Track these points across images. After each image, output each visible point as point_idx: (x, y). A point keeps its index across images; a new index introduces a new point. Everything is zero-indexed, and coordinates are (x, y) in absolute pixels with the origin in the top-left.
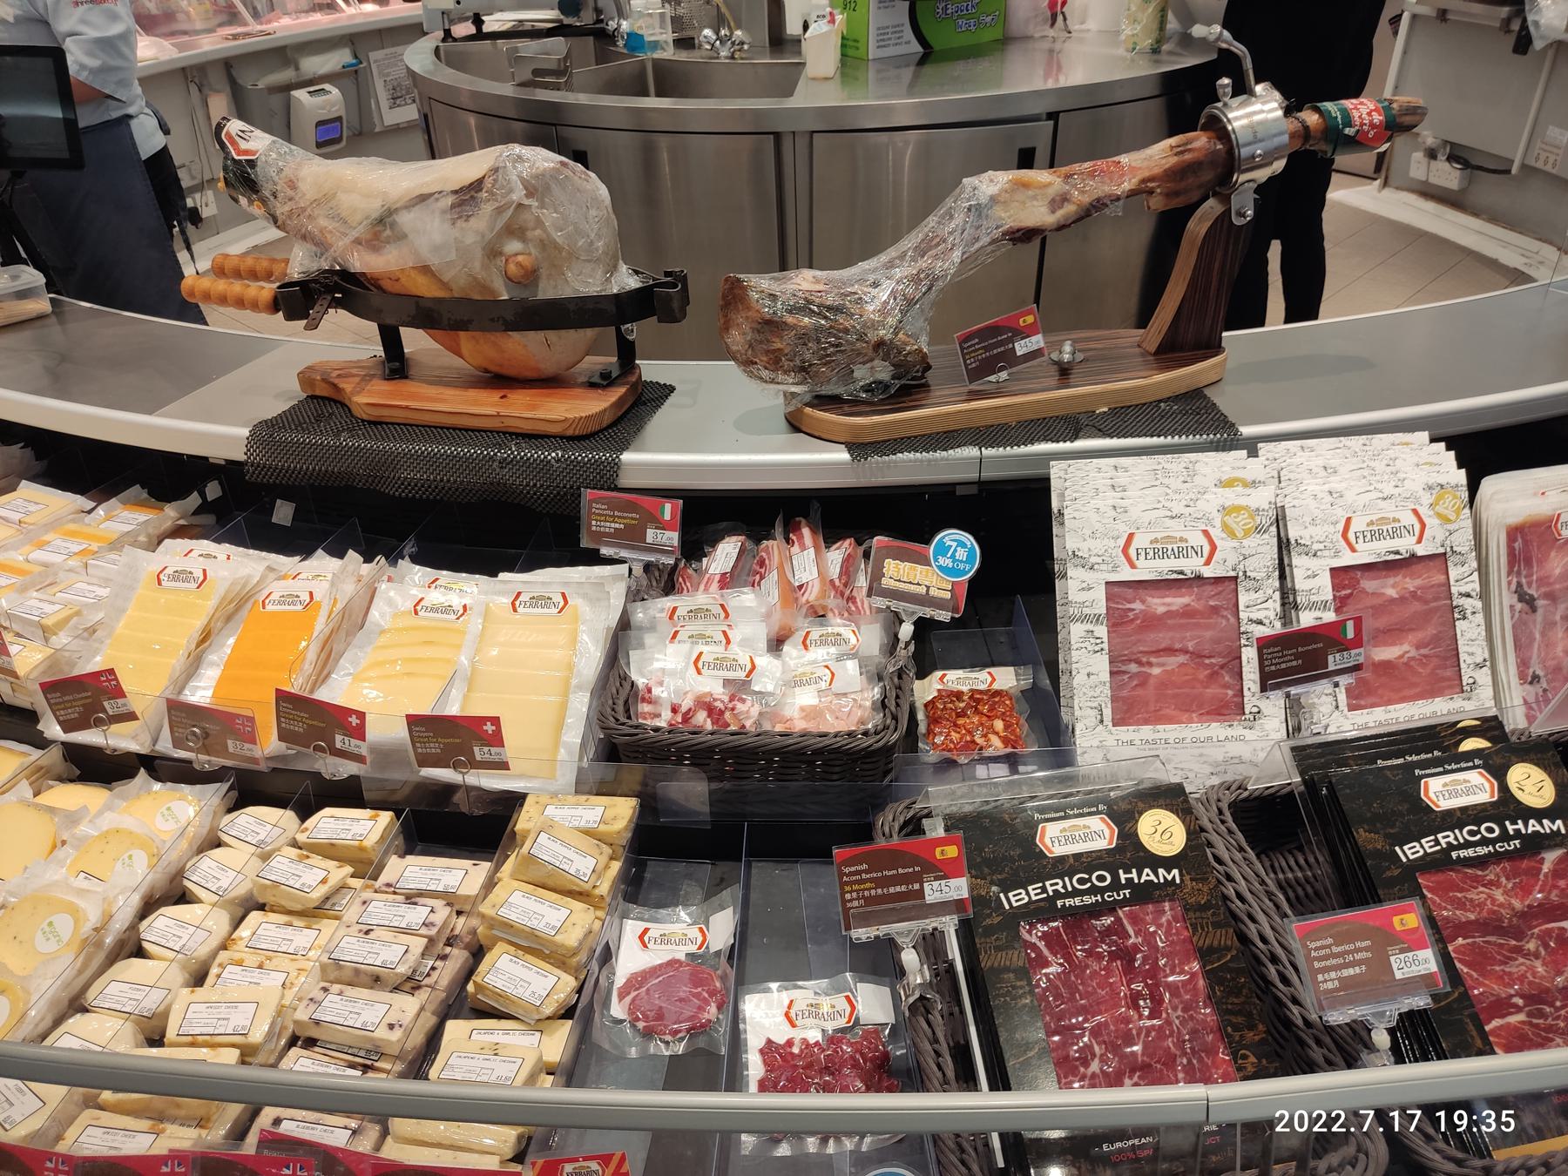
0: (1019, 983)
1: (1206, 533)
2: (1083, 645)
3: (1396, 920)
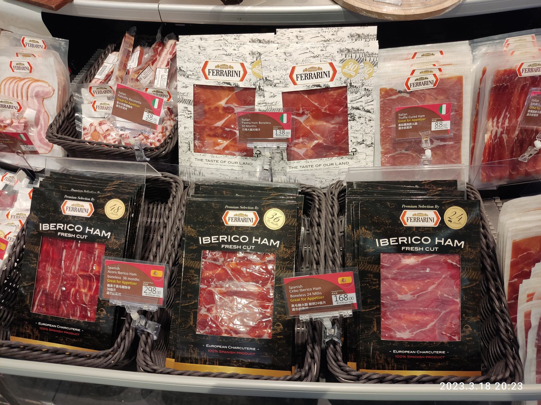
0: (195, 275)
1: (242, 65)
2: (183, 114)
3: (152, 272)
